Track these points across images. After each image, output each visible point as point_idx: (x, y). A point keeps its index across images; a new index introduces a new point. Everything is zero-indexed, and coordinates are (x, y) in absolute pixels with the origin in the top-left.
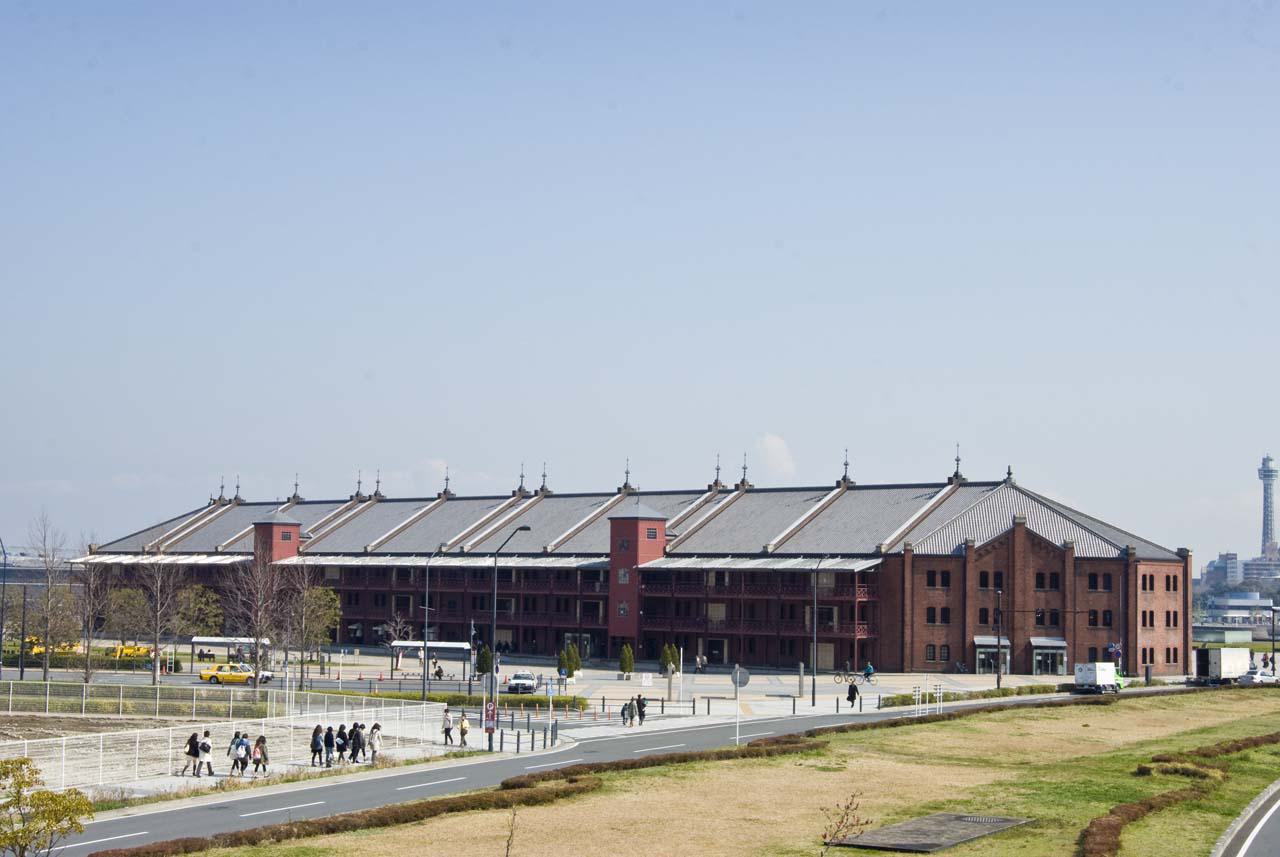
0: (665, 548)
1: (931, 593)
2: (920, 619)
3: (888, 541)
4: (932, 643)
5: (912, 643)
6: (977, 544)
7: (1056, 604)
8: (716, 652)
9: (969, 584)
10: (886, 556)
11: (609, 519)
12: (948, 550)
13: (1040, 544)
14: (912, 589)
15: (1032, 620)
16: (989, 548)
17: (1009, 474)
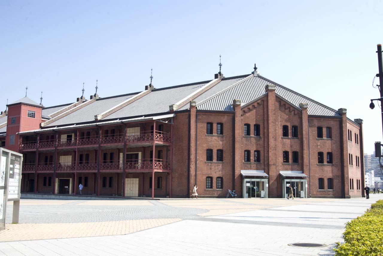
0: (40, 124)
1: (209, 138)
2: (202, 157)
3: (178, 103)
4: (210, 176)
5: (196, 175)
6: (242, 104)
7: (297, 148)
8: (67, 187)
9: (237, 132)
10: (176, 113)
12: (222, 108)
13: (285, 105)
14: (196, 135)
15: (281, 159)
16: (251, 107)
17: (255, 68)
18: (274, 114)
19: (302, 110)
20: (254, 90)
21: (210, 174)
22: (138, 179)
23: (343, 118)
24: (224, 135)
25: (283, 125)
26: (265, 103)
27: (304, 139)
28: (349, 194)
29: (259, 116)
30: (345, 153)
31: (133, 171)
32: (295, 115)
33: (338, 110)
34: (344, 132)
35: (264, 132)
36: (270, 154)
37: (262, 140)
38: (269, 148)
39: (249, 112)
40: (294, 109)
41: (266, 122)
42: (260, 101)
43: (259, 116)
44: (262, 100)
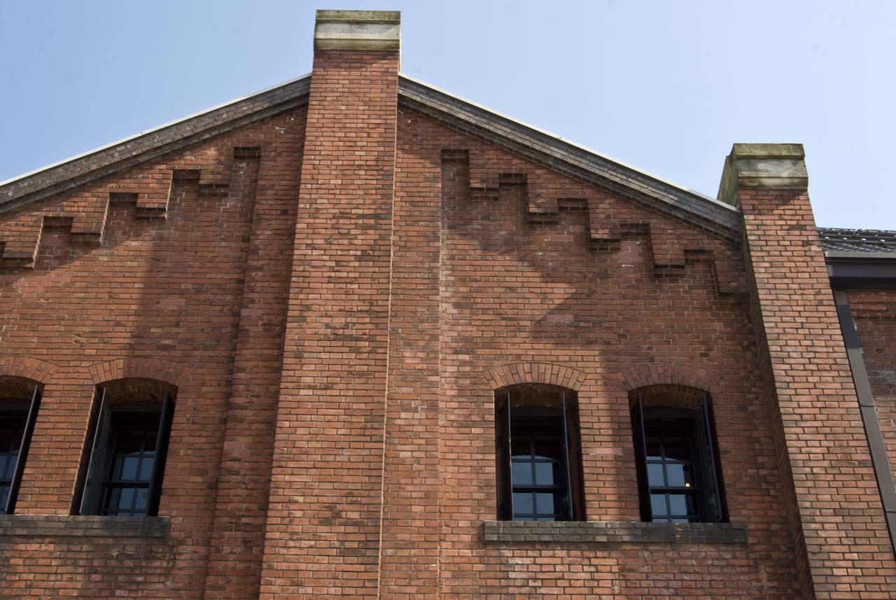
13: (516, 183)
19: (739, 216)
26: (272, 169)
27: (809, 528)
29: (171, 304)
32: (657, 272)
35: (220, 454)
37: (167, 573)
39: (63, 259)
40: (633, 216)
41: (251, 354)
42: (212, 152)
43: (171, 304)
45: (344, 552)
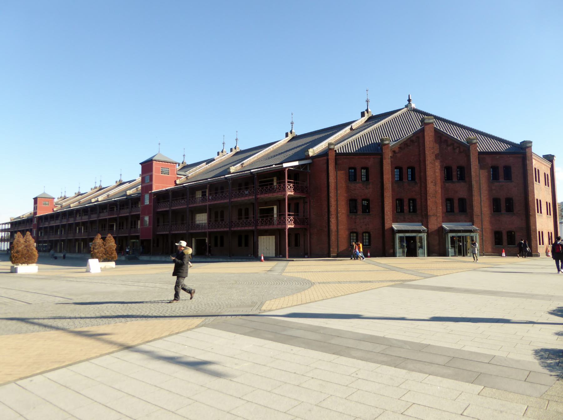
0: (175, 181)
4: (355, 230)
5: (337, 231)
11: (140, 164)
14: (336, 183)
17: (409, 100)
18: (432, 153)
20: (407, 124)
21: (354, 229)
22: (274, 237)
23: (527, 154)
24: (370, 181)
25: (445, 166)
28: (537, 251)
30: (530, 199)
31: (271, 227)
33: (520, 143)
34: (528, 171)
36: (429, 203)
38: (428, 195)
44: (417, 137)
45: (434, 185)
